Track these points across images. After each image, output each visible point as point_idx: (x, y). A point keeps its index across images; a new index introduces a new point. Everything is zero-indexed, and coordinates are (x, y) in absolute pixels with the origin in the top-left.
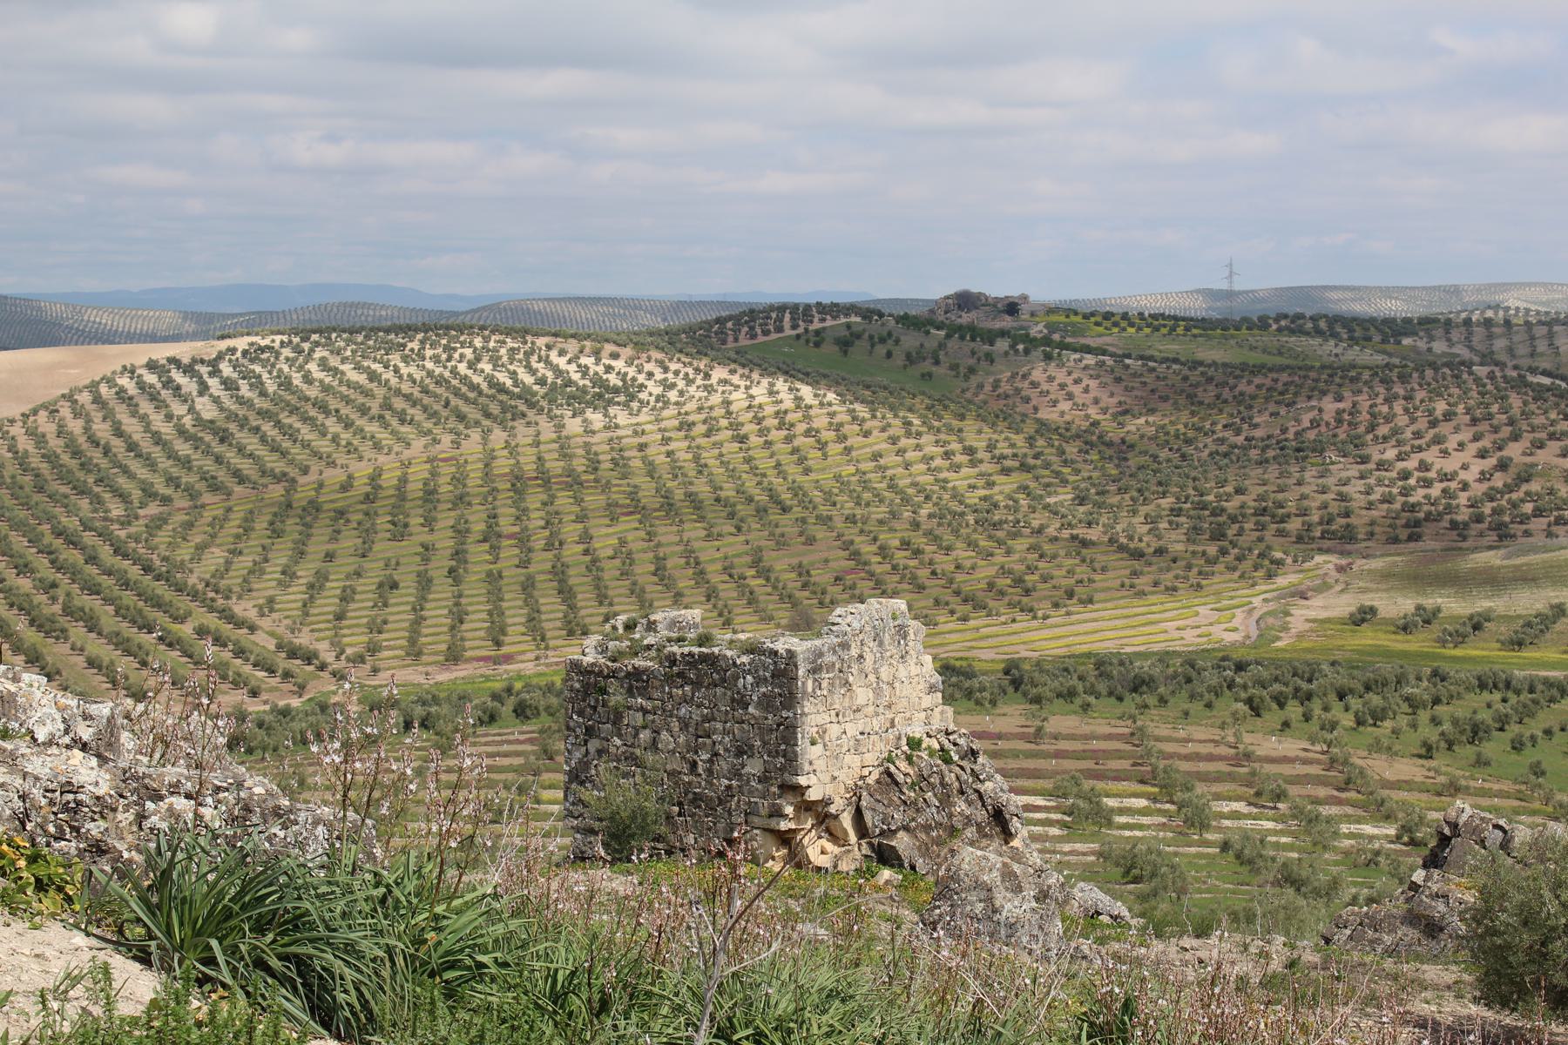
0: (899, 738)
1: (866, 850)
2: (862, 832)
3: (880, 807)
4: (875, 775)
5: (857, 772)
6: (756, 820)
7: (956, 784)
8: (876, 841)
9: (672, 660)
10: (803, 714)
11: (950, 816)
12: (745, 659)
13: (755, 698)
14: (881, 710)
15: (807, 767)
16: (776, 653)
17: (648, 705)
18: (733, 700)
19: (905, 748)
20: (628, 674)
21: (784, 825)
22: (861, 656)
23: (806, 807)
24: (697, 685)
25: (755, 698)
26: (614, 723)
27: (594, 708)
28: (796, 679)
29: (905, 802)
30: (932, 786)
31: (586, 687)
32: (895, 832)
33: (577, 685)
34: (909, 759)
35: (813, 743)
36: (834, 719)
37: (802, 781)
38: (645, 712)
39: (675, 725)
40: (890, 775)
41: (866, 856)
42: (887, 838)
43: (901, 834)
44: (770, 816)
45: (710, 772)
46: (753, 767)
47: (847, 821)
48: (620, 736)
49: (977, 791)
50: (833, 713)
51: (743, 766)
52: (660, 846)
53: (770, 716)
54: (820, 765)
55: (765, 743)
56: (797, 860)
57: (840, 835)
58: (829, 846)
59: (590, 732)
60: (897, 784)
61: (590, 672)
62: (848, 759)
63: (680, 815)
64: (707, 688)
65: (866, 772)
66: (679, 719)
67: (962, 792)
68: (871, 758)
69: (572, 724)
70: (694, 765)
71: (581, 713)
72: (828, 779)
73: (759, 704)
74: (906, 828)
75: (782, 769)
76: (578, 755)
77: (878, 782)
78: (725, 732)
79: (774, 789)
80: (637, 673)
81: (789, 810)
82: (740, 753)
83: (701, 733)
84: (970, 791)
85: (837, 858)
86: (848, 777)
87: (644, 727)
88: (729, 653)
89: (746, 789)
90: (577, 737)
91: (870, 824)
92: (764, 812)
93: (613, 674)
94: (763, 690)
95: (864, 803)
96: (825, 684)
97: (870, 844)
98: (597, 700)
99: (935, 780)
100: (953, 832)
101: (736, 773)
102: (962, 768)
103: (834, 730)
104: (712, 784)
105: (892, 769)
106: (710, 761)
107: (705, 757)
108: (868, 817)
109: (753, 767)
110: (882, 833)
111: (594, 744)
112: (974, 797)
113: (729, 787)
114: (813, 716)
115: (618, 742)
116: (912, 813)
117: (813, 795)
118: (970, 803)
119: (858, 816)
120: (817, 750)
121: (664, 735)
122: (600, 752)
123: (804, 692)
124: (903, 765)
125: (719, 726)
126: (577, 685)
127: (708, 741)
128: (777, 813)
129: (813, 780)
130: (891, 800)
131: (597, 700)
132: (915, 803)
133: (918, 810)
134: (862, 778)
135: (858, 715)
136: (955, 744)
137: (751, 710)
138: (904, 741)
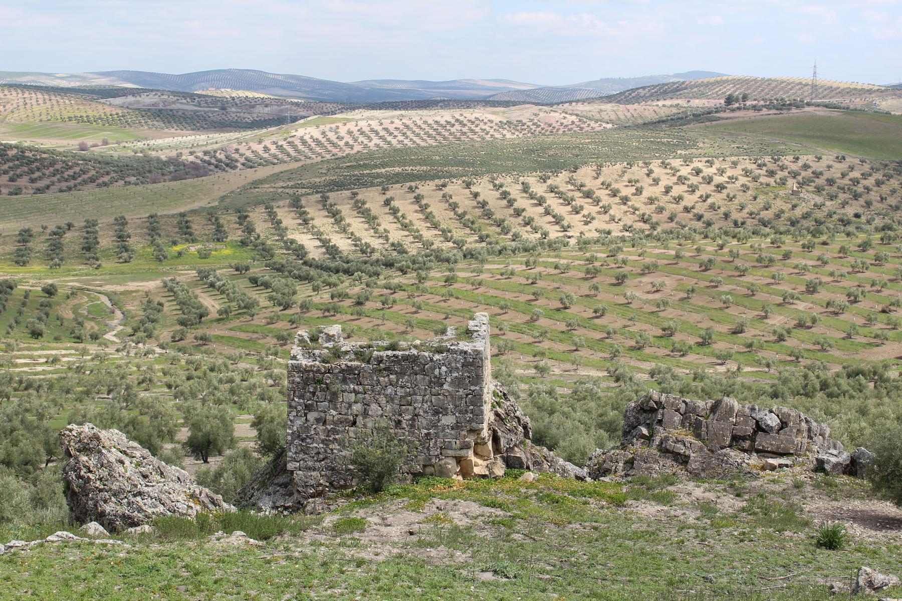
2: (497, 449)
6: (450, 452)
9: (380, 361)
12: (437, 357)
13: (449, 379)
16: (466, 352)
17: (360, 389)
18: (430, 382)
20: (342, 371)
24: (401, 374)
25: (449, 379)
26: (330, 401)
27: (314, 393)
31: (306, 382)
32: (512, 449)
33: (298, 380)
38: (356, 392)
39: (382, 400)
43: (516, 449)
45: (412, 426)
46: (448, 420)
47: (490, 444)
48: (335, 409)
51: (439, 421)
53: (461, 390)
55: (456, 406)
56: (466, 472)
59: (308, 408)
61: (309, 371)
64: (409, 376)
66: (386, 396)
69: (293, 404)
70: (398, 423)
71: (301, 397)
73: (452, 383)
74: (515, 445)
75: (470, 421)
76: (299, 422)
79: (464, 433)
80: (350, 370)
82: (436, 413)
83: (406, 402)
87: (356, 402)
88: (426, 354)
89: (441, 435)
90: (298, 412)
93: (329, 371)
94: (455, 374)
98: (315, 388)
104: (413, 433)
106: (413, 419)
108: (503, 442)
109: (448, 420)
111: (312, 416)
113: (427, 435)
115: (334, 413)
119: (496, 439)
121: (374, 406)
122: (318, 420)
125: (420, 398)
126: (298, 380)
127: (410, 407)
131: (315, 388)
137: (446, 387)
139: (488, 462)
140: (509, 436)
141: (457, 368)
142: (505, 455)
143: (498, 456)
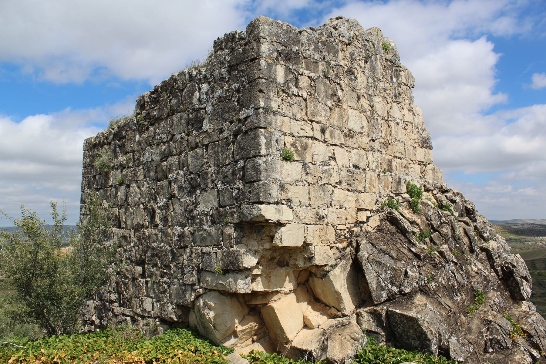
0: (399, 183)
1: (368, 323)
2: (362, 294)
3: (387, 261)
4: (375, 222)
5: (351, 216)
7: (465, 240)
8: (383, 310)
10: (268, 110)
11: (468, 276)
14: (376, 145)
15: (275, 192)
19: (406, 196)
21: (243, 286)
22: (350, 72)
23: (281, 259)
28: (256, 59)
29: (417, 256)
30: (444, 238)
32: (409, 297)
34: (413, 206)
35: (287, 158)
36: (318, 135)
37: (269, 213)
40: (393, 221)
41: (369, 333)
42: (400, 304)
43: (419, 299)
44: (226, 272)
45: (165, 219)
46: (207, 203)
47: (339, 280)
49: (483, 250)
50: (317, 127)
51: (196, 204)
52: (127, 311)
54: (298, 193)
57: (330, 300)
58: (318, 319)
60: (403, 232)
62: (339, 194)
63: (143, 275)
65: (363, 217)
67: (472, 251)
68: (368, 200)
72: (308, 215)
74: (424, 291)
77: (379, 229)
78: (182, 165)
79: (230, 230)
81: (249, 261)
82: (193, 188)
84: (478, 250)
85: (325, 338)
86: (340, 217)
91: (373, 285)
92: (217, 265)
95: (364, 253)
96: (304, 82)
97: (375, 315)
99: (446, 230)
100: (475, 296)
101: (190, 217)
102: (467, 224)
103: (319, 151)
105: (396, 214)
107: (161, 203)
108: (371, 274)
109: (207, 203)
110: (391, 298)
112: (483, 255)
113: (181, 236)
114: (284, 121)
116: (427, 269)
117: (288, 238)
118: (481, 261)
119: (357, 273)
120: (291, 171)
123: (271, 80)
124: (408, 213)
128: (233, 268)
129: (285, 214)
130: (399, 251)
132: (429, 257)
133: (435, 266)
134: (359, 223)
135: (350, 142)
136: (453, 202)
137: (206, 126)
138: (404, 189)
139: (334, 322)
140: (400, 265)
141: (222, 79)
142: (383, 310)
143: (363, 311)
